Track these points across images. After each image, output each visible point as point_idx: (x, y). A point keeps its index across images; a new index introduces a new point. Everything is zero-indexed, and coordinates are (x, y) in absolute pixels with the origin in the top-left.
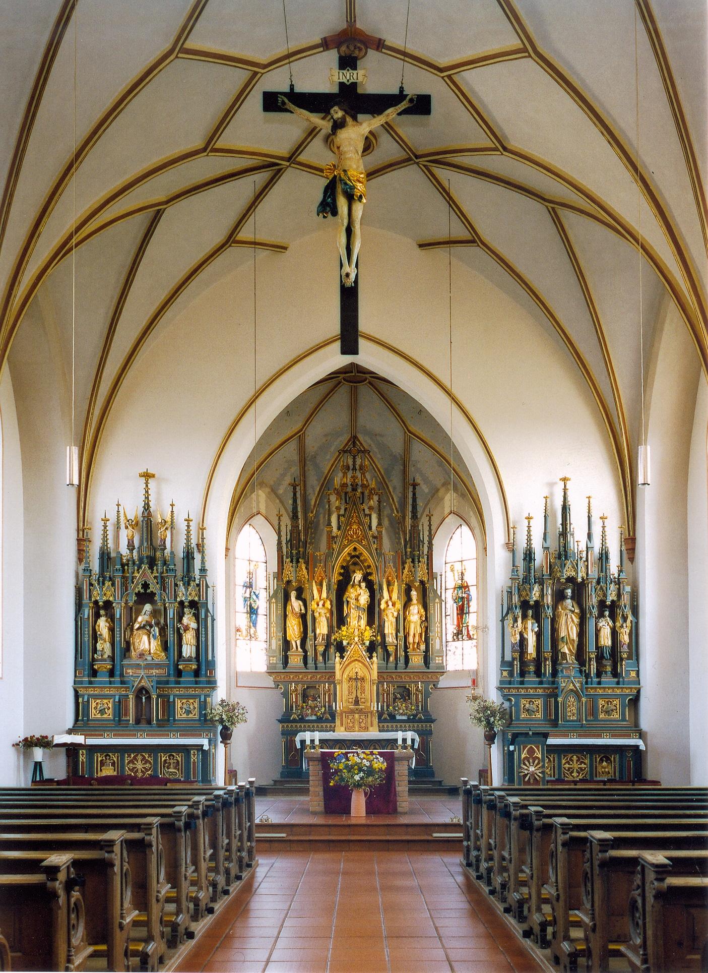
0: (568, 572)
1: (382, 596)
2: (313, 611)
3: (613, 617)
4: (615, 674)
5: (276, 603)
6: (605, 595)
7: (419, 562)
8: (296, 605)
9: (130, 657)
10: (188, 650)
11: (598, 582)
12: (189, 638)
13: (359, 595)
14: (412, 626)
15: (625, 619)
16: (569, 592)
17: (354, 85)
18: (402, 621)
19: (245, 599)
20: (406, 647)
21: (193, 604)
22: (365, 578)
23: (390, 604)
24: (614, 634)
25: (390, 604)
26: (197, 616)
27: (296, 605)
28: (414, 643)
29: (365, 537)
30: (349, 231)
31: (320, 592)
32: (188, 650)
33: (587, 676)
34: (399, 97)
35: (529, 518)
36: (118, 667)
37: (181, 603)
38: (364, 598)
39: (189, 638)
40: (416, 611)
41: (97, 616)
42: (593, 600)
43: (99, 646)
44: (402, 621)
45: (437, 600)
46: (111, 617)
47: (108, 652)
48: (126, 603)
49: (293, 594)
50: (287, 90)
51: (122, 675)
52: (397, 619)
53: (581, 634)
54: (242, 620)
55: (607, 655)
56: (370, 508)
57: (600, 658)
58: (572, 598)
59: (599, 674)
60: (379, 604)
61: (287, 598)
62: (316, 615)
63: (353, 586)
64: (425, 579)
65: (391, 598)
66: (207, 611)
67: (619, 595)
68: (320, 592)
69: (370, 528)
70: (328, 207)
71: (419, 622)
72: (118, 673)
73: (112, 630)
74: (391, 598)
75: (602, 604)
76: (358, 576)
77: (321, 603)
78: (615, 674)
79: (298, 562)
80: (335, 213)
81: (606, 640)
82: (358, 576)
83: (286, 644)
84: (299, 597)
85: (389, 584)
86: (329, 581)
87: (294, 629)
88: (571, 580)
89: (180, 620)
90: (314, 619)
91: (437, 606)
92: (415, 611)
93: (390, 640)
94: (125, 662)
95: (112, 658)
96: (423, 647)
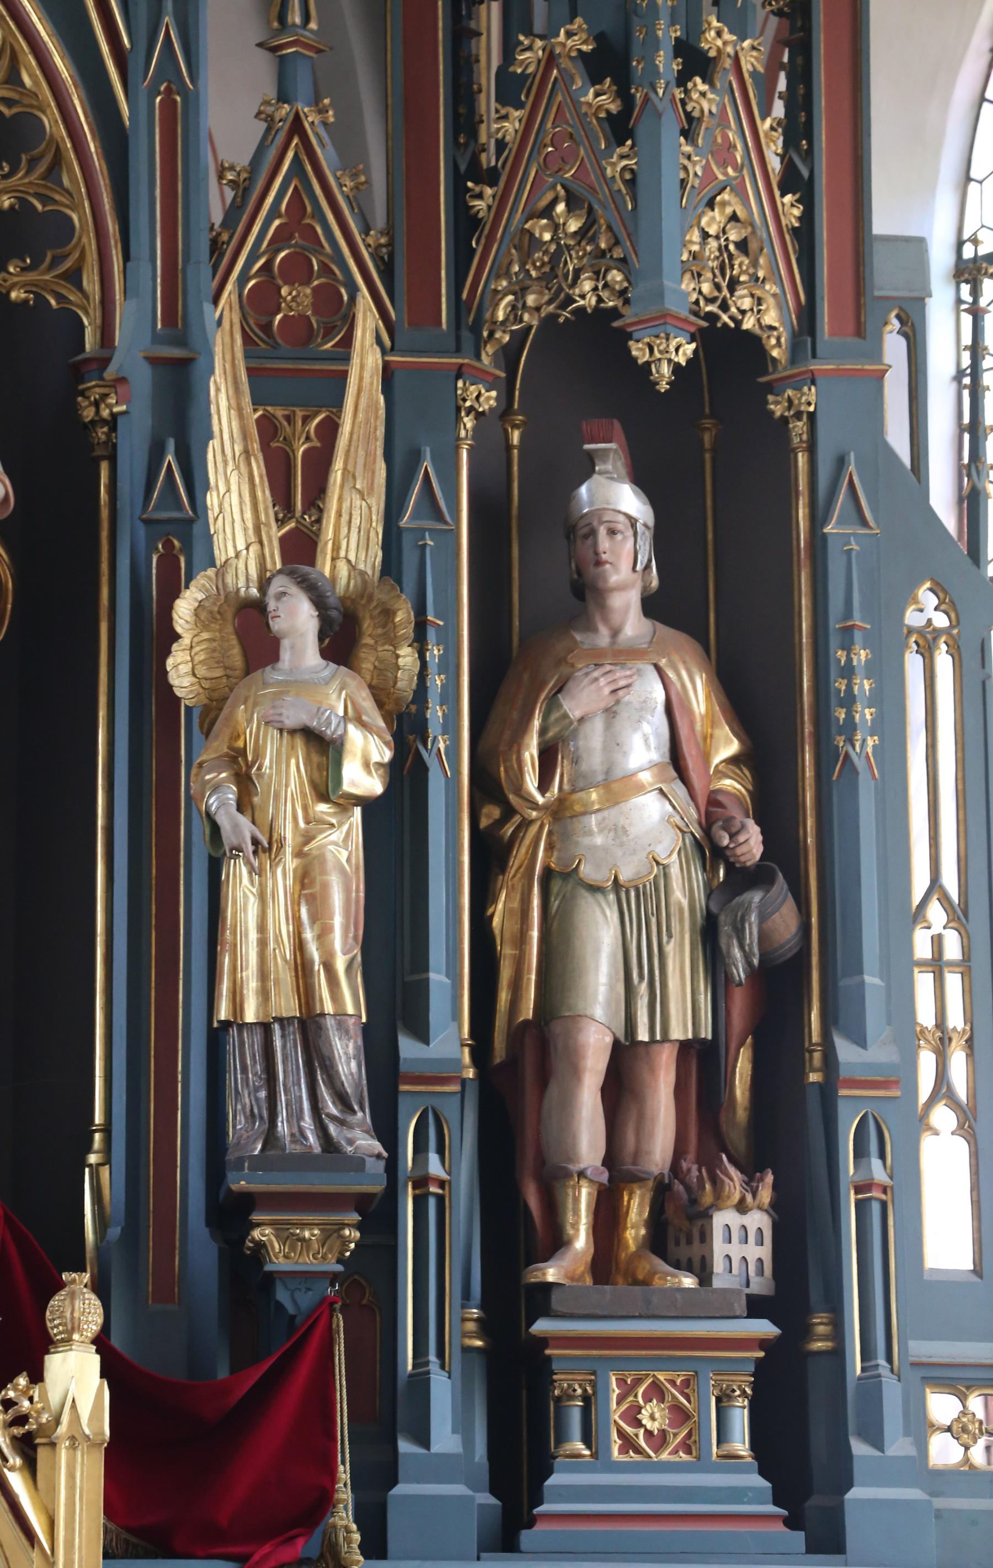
1: (183, 538)
7: (695, 62)
14: (601, 937)
18: (459, 844)
20: (514, 1228)
23: (298, 620)
25: (298, 620)
28: (619, 1170)
40: (643, 749)
44: (459, 844)
45: (926, 610)
52: (394, 825)
60: (155, 638)
64: (765, 313)
65: (300, 549)
71: (685, 890)
74: (300, 549)
85: (296, 378)
92: (639, 743)
93: (297, 1127)
96: (740, 1239)
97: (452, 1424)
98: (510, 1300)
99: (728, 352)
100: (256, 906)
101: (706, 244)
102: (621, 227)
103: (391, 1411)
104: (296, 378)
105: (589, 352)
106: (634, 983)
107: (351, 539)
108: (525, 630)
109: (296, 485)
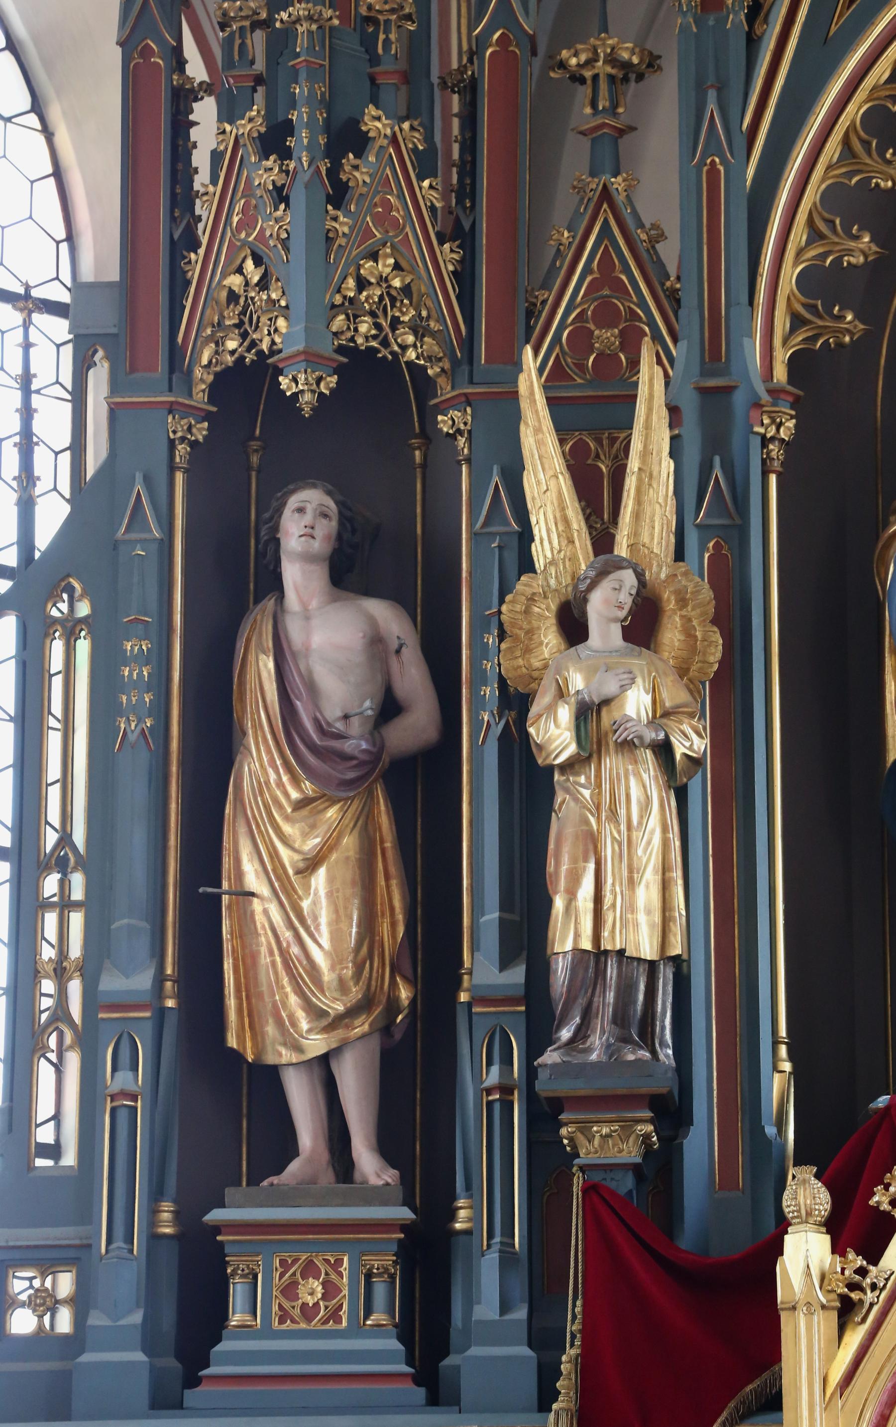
2: (516, 703)
5: (105, 632)
8: (326, 637)
27: (326, 637)
31: (598, 490)
49: (304, 525)
61: (235, 578)
62: (555, 733)
68: (598, 490)
77: (606, 607)
79: (345, 139)
83: (216, 1100)
84: (349, 570)
86: (715, 353)
87: (303, 906)
90: (530, 787)
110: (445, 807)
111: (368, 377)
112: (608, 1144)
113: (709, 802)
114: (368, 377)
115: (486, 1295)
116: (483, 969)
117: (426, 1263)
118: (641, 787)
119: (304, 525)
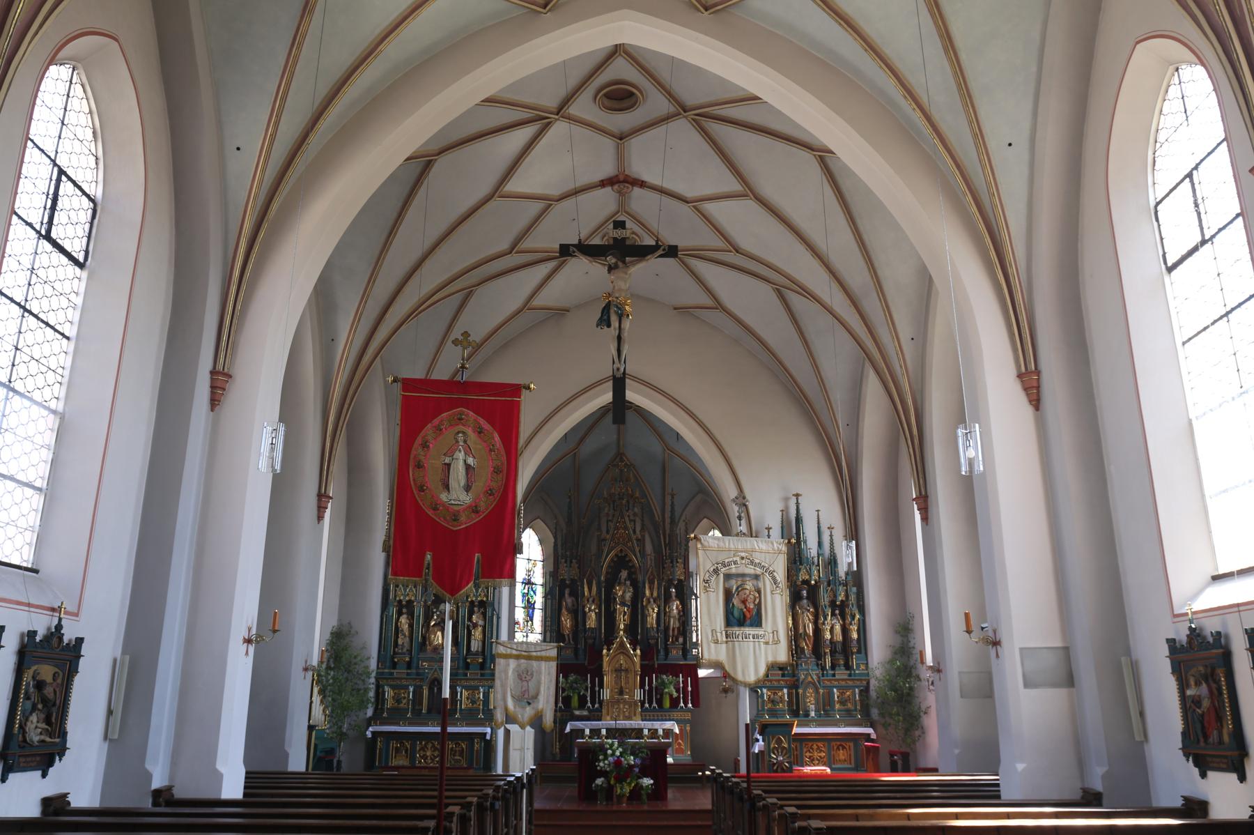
0: (803, 576)
1: (644, 593)
2: (584, 607)
3: (843, 617)
4: (848, 666)
6: (835, 596)
8: (569, 600)
9: (425, 651)
10: (475, 645)
11: (829, 585)
12: (477, 633)
13: (623, 592)
15: (853, 617)
16: (805, 593)
17: (624, 239)
19: (524, 595)
21: (482, 604)
22: (629, 575)
24: (845, 631)
26: (484, 614)
27: (569, 600)
29: (630, 540)
30: (619, 338)
32: (475, 645)
33: (823, 668)
34: (657, 247)
35: (769, 529)
36: (415, 660)
37: (472, 602)
38: (628, 596)
39: (477, 633)
41: (400, 614)
42: (824, 599)
43: (400, 642)
46: (411, 615)
47: (407, 646)
48: (425, 602)
49: (567, 591)
50: (576, 242)
51: (418, 667)
52: (658, 614)
53: (817, 631)
54: (520, 614)
55: (839, 648)
56: (635, 515)
57: (833, 653)
58: (808, 598)
59: (833, 667)
61: (562, 595)
63: (619, 584)
66: (494, 610)
67: (847, 596)
69: (634, 532)
70: (604, 321)
72: (414, 665)
73: (411, 626)
75: (833, 604)
76: (624, 574)
78: (848, 666)
80: (609, 326)
81: (839, 638)
82: (624, 574)
85: (652, 583)
87: (567, 622)
88: (806, 582)
89: (470, 619)
90: (584, 614)
91: (693, 602)
92: (675, 606)
94: (421, 655)
95: (410, 652)
96: (681, 640)
97: (662, 653)
98: (666, 645)
99: (680, 581)
100: (649, 619)
101: (679, 573)
102: (673, 573)
103: (658, 652)
104: (652, 583)
105: (670, 583)
106: (674, 623)
107: (655, 594)
108: (668, 599)
109: (651, 590)
110: (578, 615)
111: (572, 580)
112: (590, 641)
113: (598, 615)
114: (572, 580)
115: (581, 652)
116: (580, 627)
117: (576, 651)
118: (593, 614)
119: (567, 591)
